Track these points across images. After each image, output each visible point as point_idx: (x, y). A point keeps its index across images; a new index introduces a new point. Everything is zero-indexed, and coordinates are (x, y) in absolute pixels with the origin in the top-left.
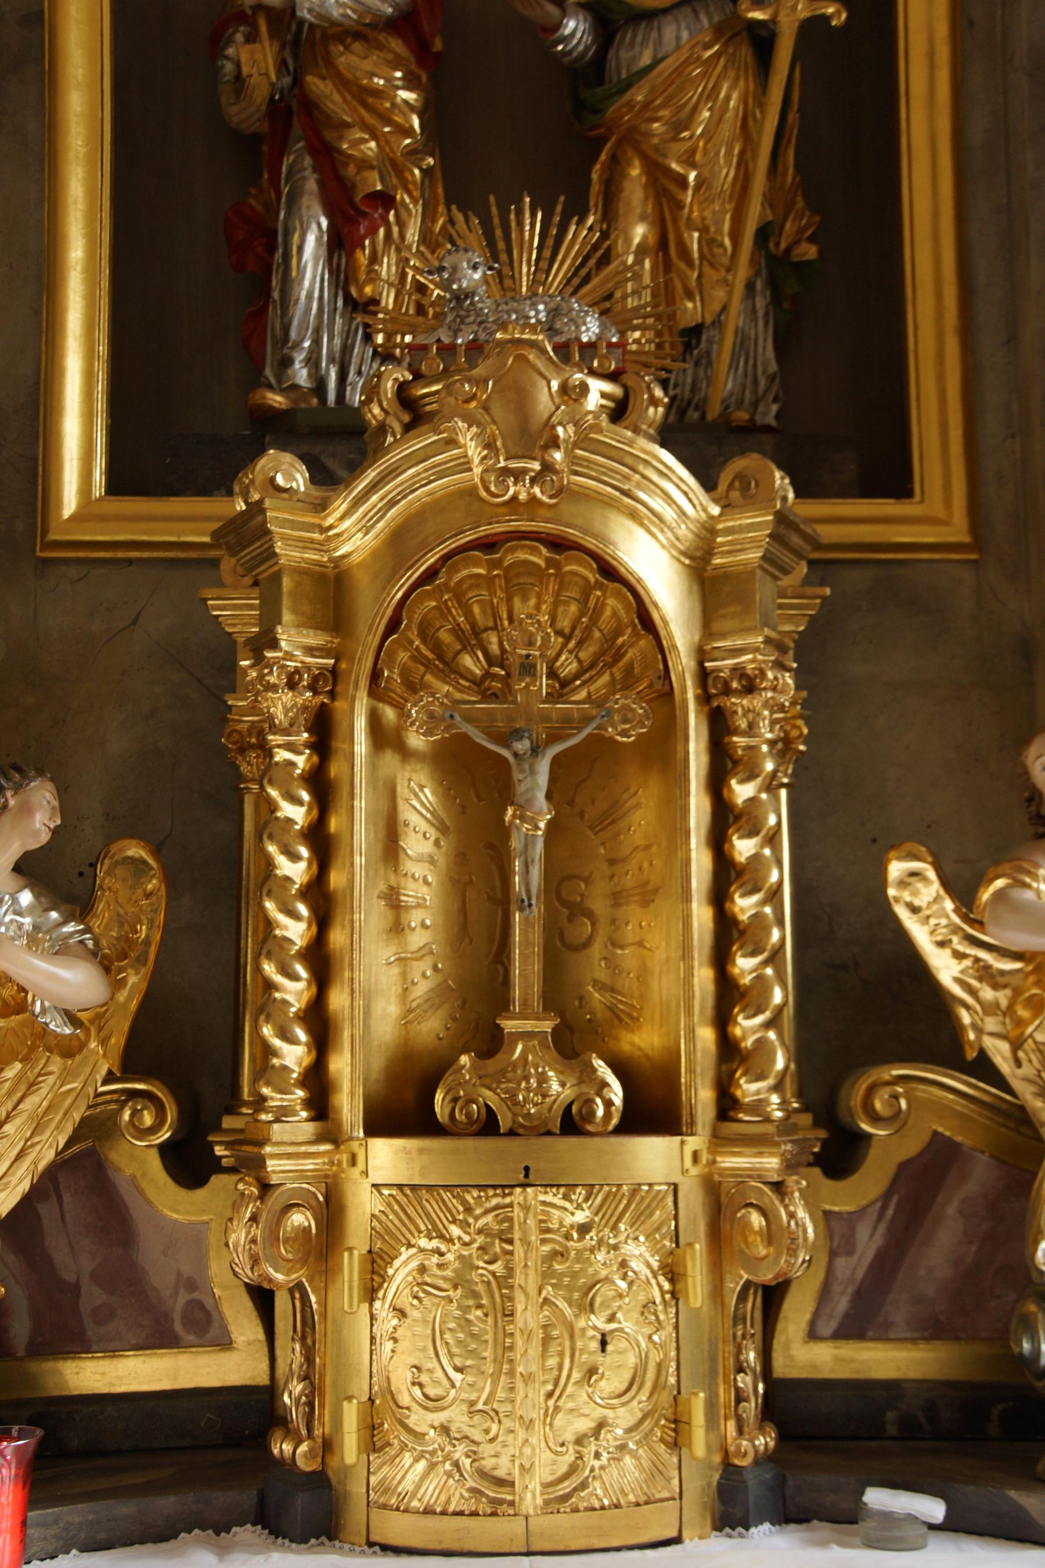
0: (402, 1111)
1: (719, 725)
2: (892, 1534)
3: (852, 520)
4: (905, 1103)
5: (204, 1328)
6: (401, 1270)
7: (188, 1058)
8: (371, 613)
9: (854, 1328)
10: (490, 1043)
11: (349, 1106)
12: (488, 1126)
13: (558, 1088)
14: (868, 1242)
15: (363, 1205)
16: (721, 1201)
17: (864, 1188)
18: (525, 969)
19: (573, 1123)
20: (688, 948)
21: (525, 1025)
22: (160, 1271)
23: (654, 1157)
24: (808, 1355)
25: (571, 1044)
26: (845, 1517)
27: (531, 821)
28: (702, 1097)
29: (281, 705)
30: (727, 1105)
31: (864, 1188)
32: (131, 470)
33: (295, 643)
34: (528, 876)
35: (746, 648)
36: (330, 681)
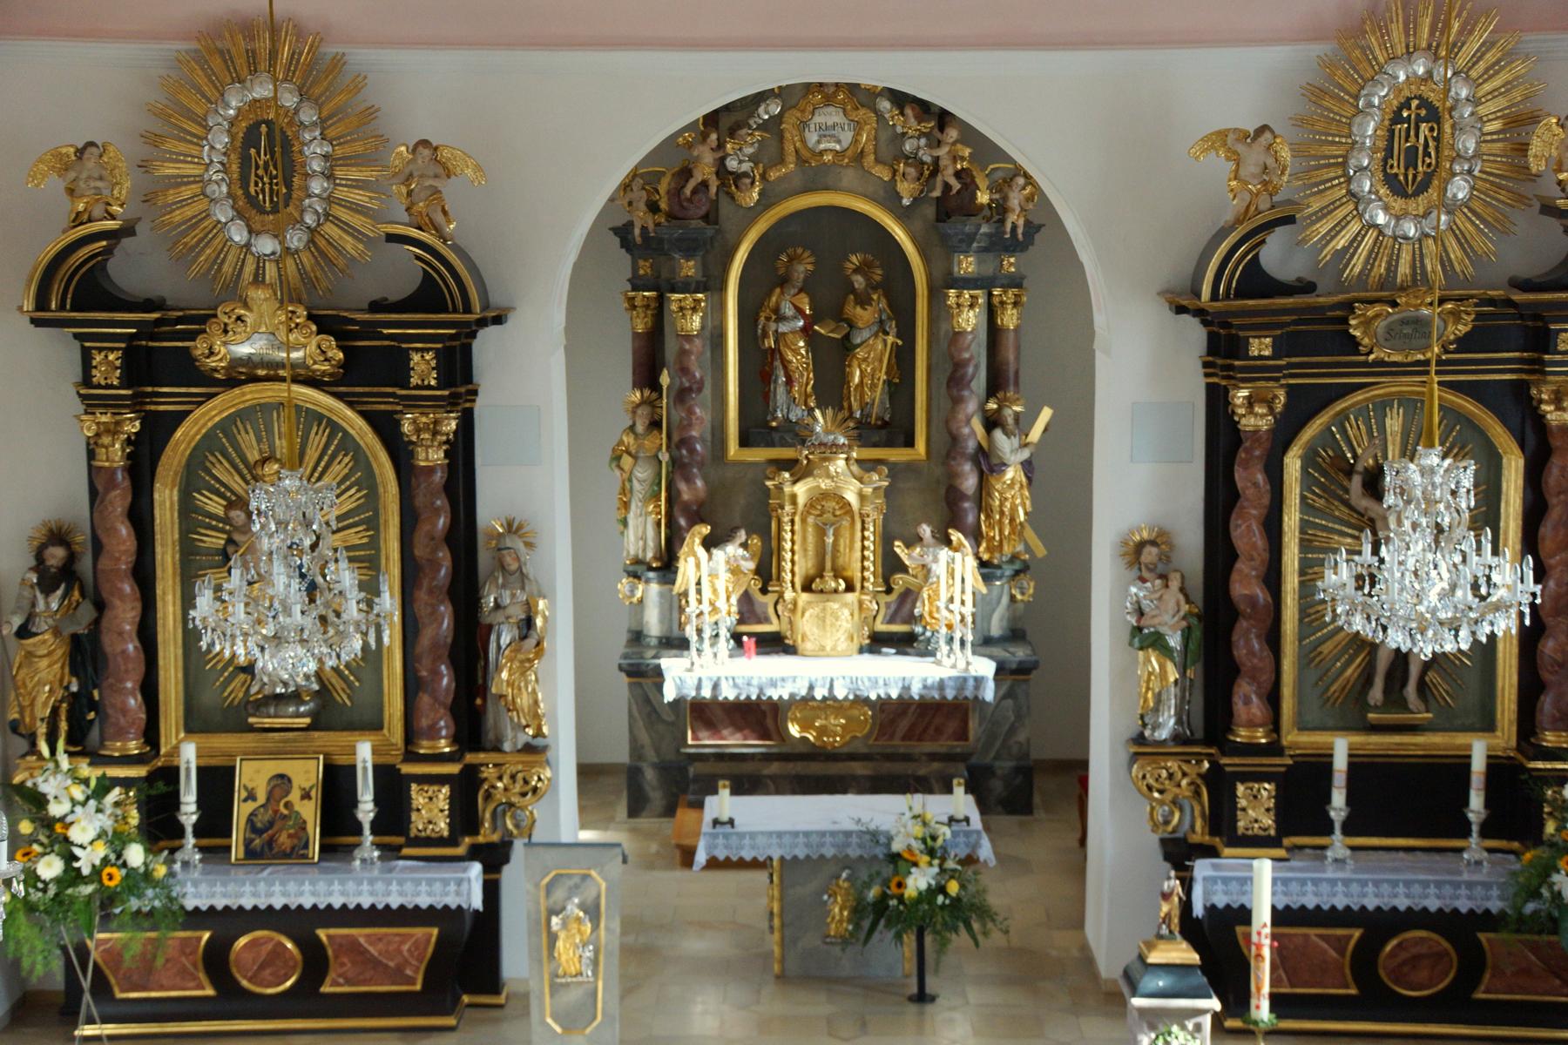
0: (807, 588)
1: (863, 522)
2: (887, 654)
3: (897, 455)
4: (899, 581)
5: (767, 620)
6: (807, 614)
7: (766, 572)
8: (801, 500)
9: (891, 621)
10: (822, 577)
11: (798, 586)
12: (822, 591)
13: (833, 585)
14: (893, 607)
15: (800, 604)
16: (861, 603)
17: (893, 597)
18: (828, 565)
19: (836, 591)
20: (859, 552)
21: (828, 574)
22: (758, 610)
23: (851, 597)
24: (881, 627)
25: (836, 577)
26: (879, 653)
27: (830, 540)
28: (858, 586)
29: (786, 519)
30: (863, 587)
31: (893, 597)
32: (744, 442)
33: (788, 508)
34: (829, 549)
35: (868, 509)
36: (794, 514)
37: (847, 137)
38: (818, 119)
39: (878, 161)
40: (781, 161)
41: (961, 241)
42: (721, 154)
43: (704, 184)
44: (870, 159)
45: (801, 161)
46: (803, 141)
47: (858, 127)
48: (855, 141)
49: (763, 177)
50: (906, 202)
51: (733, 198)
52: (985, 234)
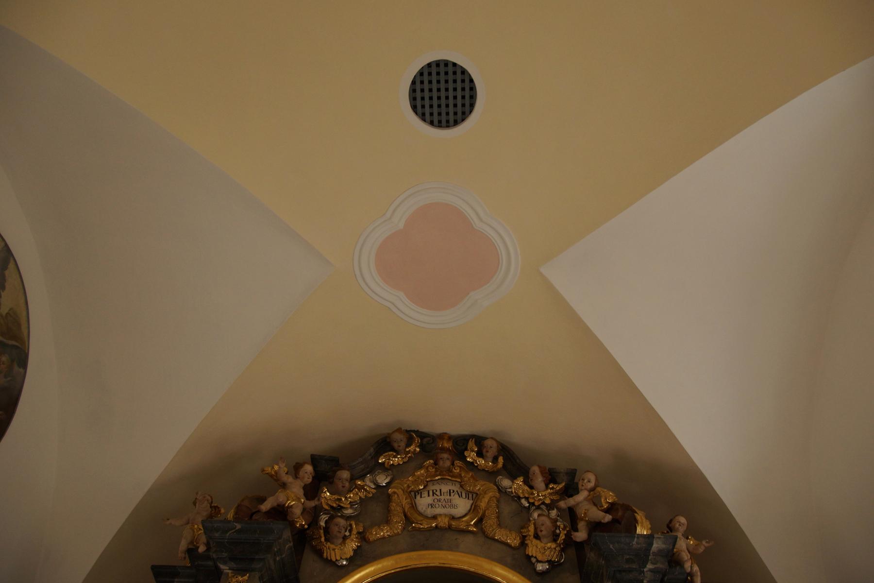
37: (462, 506)
38: (431, 487)
39: (500, 526)
40: (387, 522)
41: (628, 561)
42: (312, 504)
43: (281, 513)
44: (490, 523)
45: (408, 520)
46: (414, 506)
47: (475, 496)
48: (474, 509)
49: (362, 536)
50: (540, 567)
51: (319, 553)
52: (660, 552)
